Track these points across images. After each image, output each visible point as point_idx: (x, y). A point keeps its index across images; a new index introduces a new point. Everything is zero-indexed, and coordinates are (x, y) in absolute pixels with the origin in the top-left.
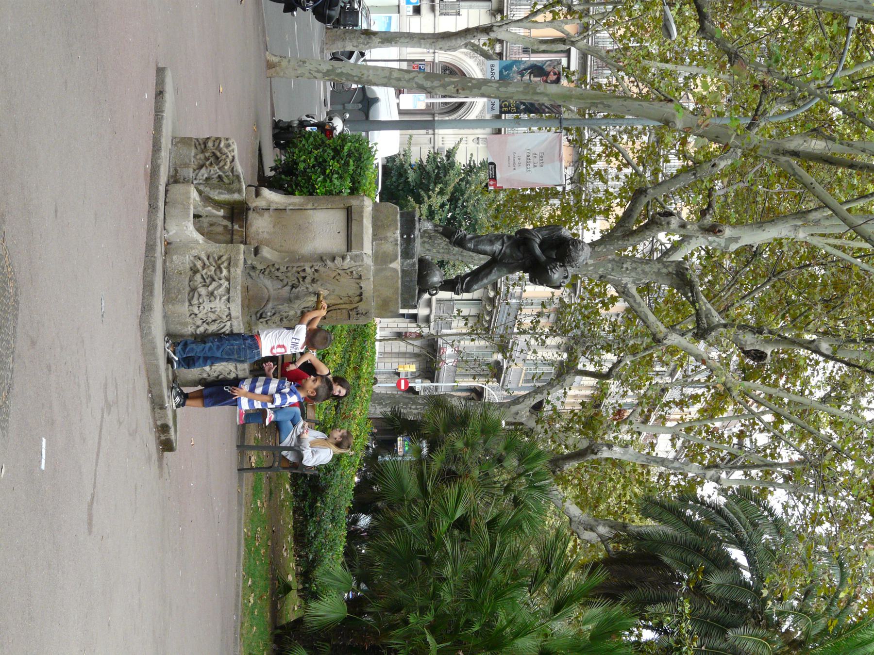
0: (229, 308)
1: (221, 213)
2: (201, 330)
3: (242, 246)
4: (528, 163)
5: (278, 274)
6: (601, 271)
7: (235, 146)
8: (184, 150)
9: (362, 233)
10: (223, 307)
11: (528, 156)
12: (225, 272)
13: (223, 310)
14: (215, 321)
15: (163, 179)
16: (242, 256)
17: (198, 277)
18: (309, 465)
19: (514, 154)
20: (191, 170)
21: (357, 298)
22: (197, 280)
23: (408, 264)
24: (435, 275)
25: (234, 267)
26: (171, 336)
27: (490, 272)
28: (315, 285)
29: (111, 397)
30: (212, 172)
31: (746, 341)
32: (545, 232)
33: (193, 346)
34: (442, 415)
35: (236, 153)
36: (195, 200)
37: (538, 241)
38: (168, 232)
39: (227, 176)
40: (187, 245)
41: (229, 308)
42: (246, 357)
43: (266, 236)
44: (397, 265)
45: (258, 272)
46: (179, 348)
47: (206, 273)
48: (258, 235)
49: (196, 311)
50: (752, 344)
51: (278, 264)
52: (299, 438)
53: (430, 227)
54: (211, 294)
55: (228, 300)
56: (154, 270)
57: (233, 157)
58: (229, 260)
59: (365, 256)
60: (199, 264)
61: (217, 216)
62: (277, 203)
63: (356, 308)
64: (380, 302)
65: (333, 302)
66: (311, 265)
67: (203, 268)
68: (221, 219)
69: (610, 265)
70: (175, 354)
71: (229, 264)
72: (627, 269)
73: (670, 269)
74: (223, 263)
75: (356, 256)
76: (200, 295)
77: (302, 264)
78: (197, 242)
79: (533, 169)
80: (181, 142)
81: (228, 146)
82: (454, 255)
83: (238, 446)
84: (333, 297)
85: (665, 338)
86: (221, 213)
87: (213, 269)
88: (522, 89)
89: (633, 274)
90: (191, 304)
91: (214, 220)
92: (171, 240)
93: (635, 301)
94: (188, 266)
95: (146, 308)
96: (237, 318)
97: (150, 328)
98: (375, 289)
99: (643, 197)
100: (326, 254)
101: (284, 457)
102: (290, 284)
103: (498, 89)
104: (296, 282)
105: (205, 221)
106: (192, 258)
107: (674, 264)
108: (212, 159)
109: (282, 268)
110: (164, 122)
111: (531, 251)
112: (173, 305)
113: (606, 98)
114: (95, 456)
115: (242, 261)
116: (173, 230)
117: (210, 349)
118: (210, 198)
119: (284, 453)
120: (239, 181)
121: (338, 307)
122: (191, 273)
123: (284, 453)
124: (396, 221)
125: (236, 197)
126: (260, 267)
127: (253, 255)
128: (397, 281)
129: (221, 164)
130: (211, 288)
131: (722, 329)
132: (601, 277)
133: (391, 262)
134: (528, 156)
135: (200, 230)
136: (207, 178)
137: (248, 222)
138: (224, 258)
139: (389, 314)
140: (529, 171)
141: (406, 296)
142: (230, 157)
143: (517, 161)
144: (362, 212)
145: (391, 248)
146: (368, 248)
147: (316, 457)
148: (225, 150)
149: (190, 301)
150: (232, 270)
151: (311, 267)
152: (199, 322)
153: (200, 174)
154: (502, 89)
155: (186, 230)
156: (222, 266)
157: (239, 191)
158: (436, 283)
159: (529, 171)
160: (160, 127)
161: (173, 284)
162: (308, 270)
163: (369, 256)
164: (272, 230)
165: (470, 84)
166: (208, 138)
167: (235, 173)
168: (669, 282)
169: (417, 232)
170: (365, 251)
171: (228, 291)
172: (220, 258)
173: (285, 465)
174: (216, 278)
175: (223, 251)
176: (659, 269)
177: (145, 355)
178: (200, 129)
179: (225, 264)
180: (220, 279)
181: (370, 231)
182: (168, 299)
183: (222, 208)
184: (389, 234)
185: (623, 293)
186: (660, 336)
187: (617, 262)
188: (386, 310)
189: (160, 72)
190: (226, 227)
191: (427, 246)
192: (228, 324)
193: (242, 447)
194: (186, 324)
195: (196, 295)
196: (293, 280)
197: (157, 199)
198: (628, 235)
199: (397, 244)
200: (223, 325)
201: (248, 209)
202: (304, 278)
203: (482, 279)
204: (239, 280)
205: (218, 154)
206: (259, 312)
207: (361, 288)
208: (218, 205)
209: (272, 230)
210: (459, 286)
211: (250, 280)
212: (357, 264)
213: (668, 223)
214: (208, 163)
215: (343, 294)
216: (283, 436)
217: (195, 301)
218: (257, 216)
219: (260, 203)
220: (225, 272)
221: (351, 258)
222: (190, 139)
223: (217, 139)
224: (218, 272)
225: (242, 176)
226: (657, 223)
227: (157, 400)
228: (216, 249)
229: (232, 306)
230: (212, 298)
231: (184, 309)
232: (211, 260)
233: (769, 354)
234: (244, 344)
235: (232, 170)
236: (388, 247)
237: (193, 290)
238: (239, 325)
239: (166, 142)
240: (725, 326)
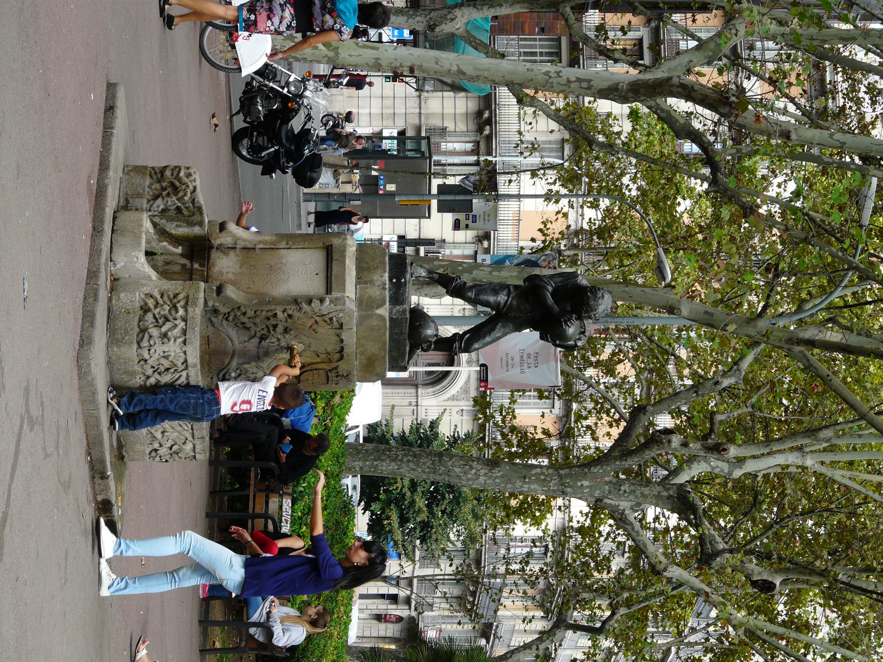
0: (185, 353)
1: (179, 250)
2: (152, 381)
3: (202, 284)
4: (522, 364)
5: (245, 320)
6: (597, 494)
7: (196, 176)
8: (137, 179)
9: (344, 274)
10: (178, 351)
11: (522, 357)
12: (181, 312)
13: (177, 354)
14: (167, 370)
15: (111, 203)
16: (202, 295)
17: (149, 317)
18: (281, 644)
19: (507, 354)
20: (145, 201)
21: (337, 356)
22: (149, 319)
23: (398, 311)
24: (429, 328)
25: (192, 305)
26: (118, 390)
27: (494, 329)
28: (287, 336)
29: (35, 411)
30: (170, 203)
31: (753, 571)
32: (558, 279)
33: (143, 397)
34: (426, 653)
35: (198, 183)
36: (147, 232)
37: (550, 288)
38: (115, 265)
39: (187, 208)
40: (138, 282)
41: (185, 353)
42: (203, 414)
43: (231, 276)
44: (384, 311)
45: (220, 317)
46: (125, 399)
47: (159, 313)
48: (222, 275)
49: (146, 356)
50: (760, 573)
51: (245, 306)
52: (269, 613)
53: (424, 274)
54: (165, 335)
55: (184, 342)
56: (96, 299)
57: (195, 188)
58: (187, 298)
59: (347, 299)
60: (151, 303)
61: (174, 254)
62: (244, 240)
63: (336, 368)
64: (364, 362)
65: (309, 360)
66: (283, 308)
67: (156, 307)
68: (179, 257)
69: (607, 488)
70: (119, 406)
71: (187, 303)
72: (625, 491)
73: (671, 493)
74: (179, 302)
75: (337, 299)
76: (151, 337)
77: (273, 307)
78: (149, 278)
79: (527, 370)
80: (133, 170)
81: (189, 175)
82: (440, 475)
83: (200, 621)
84: (308, 353)
85: (665, 570)
86: (179, 250)
87: (167, 308)
88: (515, 274)
89: (632, 497)
90: (140, 347)
91: (170, 258)
92: (119, 275)
93: (633, 529)
94: (138, 305)
95: (85, 342)
96: (195, 366)
97: (89, 365)
99: (642, 415)
100: (302, 297)
101: (252, 637)
102: (258, 335)
103: (490, 273)
104: (265, 332)
105: (160, 259)
106: (143, 296)
107: (675, 487)
108: (169, 190)
109: (249, 311)
110: (114, 139)
111: (542, 301)
112: (119, 347)
113: (606, 284)
114: (9, 468)
115: (201, 301)
116: (121, 261)
117: (162, 400)
118: (166, 232)
119: (252, 630)
120: (201, 213)
121: (314, 366)
122: (141, 312)
123: (252, 630)
124: (384, 263)
125: (197, 230)
126: (223, 310)
127: (214, 295)
128: (385, 332)
129: (180, 194)
130: (164, 329)
131: (727, 555)
132: (596, 501)
133: (378, 308)
134: (522, 357)
135: (154, 267)
136: (162, 210)
137: (211, 261)
138: (181, 296)
139: (375, 378)
140: (522, 372)
141: (394, 354)
142: (191, 187)
143: (510, 362)
144: (345, 251)
145: (378, 293)
146: (351, 290)
147: (287, 635)
148: (186, 180)
149: (138, 343)
150: (190, 309)
151: (283, 312)
152: (150, 372)
153: (155, 205)
154: (495, 273)
155: (134, 263)
156: (178, 305)
157: (201, 224)
158: (431, 336)
159: (522, 372)
160: (110, 144)
161: (119, 324)
162: (280, 315)
163: (351, 300)
164: (239, 270)
165: (460, 268)
166: (166, 167)
167: (196, 205)
168: (670, 507)
169: (408, 276)
170: (347, 294)
171: (184, 332)
172: (176, 296)
173: (253, 645)
174: (171, 318)
175: (180, 288)
176: (659, 492)
177: (83, 402)
178: (155, 157)
179: (182, 303)
180: (175, 319)
181: (354, 273)
182: (114, 337)
183: (179, 244)
184: (375, 278)
185: (621, 519)
186: (660, 567)
187: (614, 484)
188: (371, 373)
189: (111, 87)
190: (183, 266)
191: (411, 464)
192: (184, 374)
193: (205, 622)
194: (133, 374)
195: (146, 336)
196: (260, 330)
197: (102, 222)
198: (626, 455)
199: (384, 288)
200: (178, 375)
201: (211, 247)
202: (275, 326)
203: (484, 337)
204: (198, 320)
205: (177, 184)
206: (220, 365)
207: (342, 341)
208: (176, 240)
209: (239, 270)
210: (457, 344)
211: (211, 328)
212: (338, 308)
213: (669, 441)
214: (164, 193)
215: (321, 350)
216: (251, 611)
217: (145, 343)
218: (221, 255)
219: (224, 239)
220: (181, 312)
221: (331, 302)
222: (146, 167)
223: (176, 167)
224: (173, 312)
225: (204, 208)
226: (657, 441)
227: (98, 466)
228: (172, 286)
229: (189, 349)
230: (165, 340)
231: (131, 352)
232: (165, 298)
233: (778, 584)
234: (203, 398)
235: (193, 202)
236: (374, 292)
237: (143, 331)
238: (197, 376)
239: (115, 175)
240: (731, 551)
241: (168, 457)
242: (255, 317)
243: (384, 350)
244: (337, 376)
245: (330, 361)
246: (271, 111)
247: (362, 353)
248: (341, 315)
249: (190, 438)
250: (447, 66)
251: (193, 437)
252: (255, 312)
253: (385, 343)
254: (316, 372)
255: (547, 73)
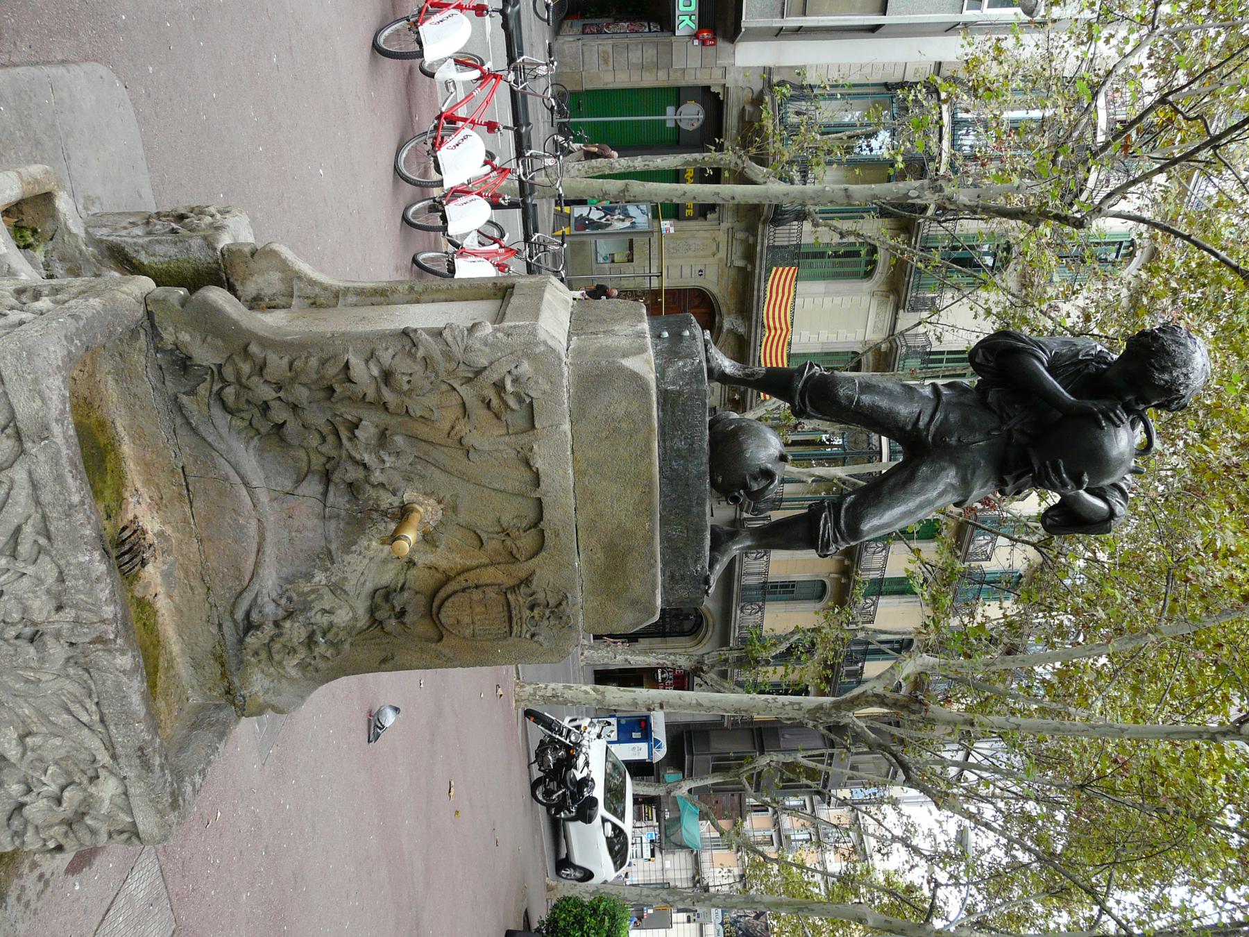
21: (527, 541)
23: (680, 374)
63: (527, 581)
64: (600, 556)
98: (585, 496)
128: (649, 451)
133: (624, 356)
141: (677, 532)
211: (185, 437)
215: (485, 523)
241: (58, 830)
242: (292, 380)
243: (649, 512)
244: (532, 608)
245: (513, 558)
246: (558, 760)
247: (592, 527)
248: (526, 368)
249: (104, 758)
250: (688, 700)
251: (114, 757)
252: (291, 364)
253: (650, 485)
254: (477, 595)
255: (766, 700)
